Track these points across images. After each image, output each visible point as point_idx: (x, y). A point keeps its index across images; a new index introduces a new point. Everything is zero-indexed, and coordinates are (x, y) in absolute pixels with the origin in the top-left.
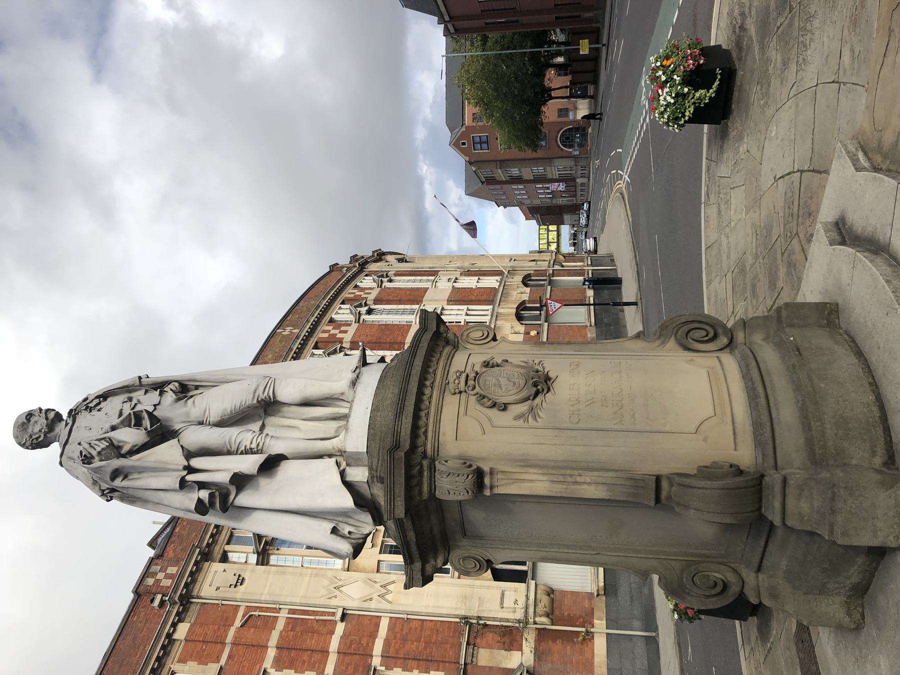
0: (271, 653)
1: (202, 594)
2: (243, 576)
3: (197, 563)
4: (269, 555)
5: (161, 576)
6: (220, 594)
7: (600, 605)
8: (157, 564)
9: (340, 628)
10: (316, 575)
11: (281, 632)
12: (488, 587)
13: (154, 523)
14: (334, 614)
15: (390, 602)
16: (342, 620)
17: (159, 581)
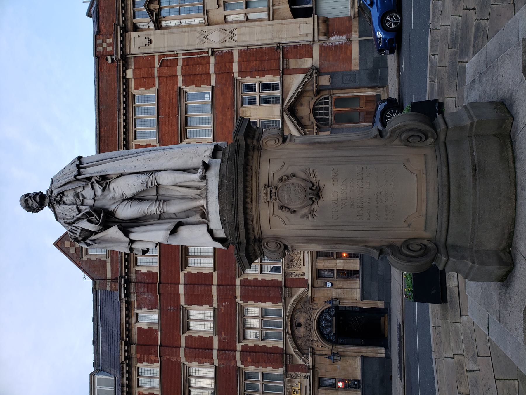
0: (180, 79)
1: (132, 53)
2: (150, 38)
3: (121, 35)
4: (160, 22)
5: (104, 45)
6: (142, 51)
7: (355, 24)
8: (99, 38)
9: (213, 60)
10: (191, 31)
11: (182, 67)
12: (290, 23)
13: (84, 2)
14: (207, 52)
15: (236, 41)
16: (212, 55)
17: (105, 48)
